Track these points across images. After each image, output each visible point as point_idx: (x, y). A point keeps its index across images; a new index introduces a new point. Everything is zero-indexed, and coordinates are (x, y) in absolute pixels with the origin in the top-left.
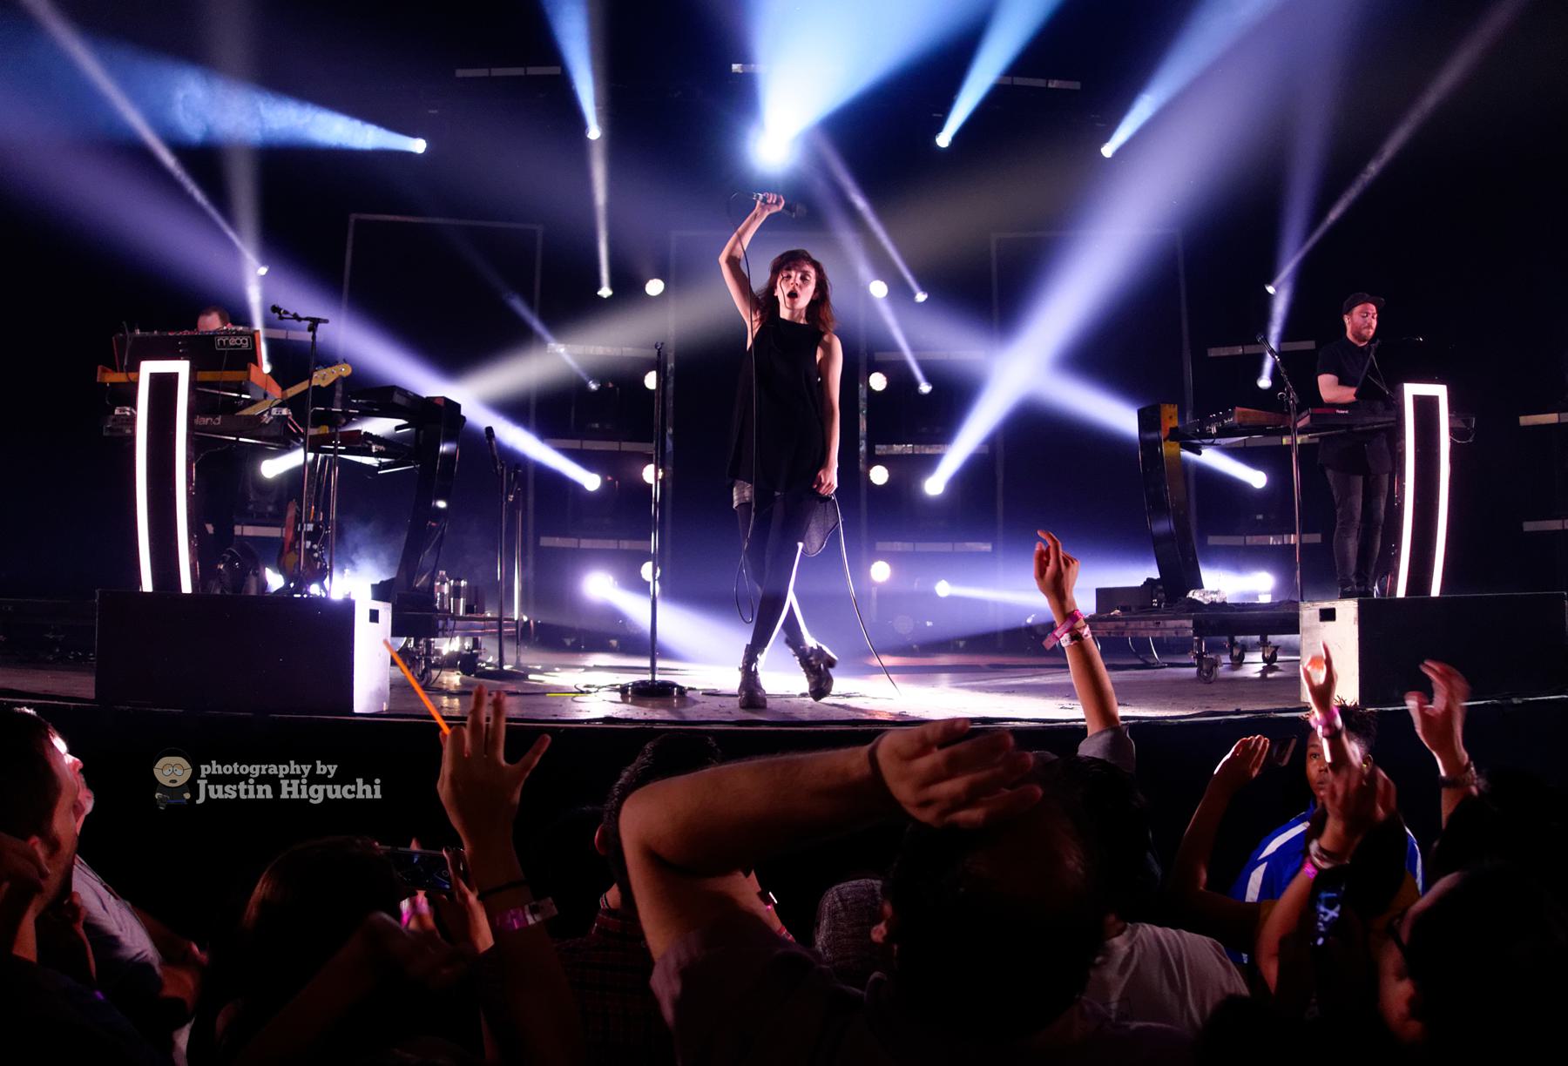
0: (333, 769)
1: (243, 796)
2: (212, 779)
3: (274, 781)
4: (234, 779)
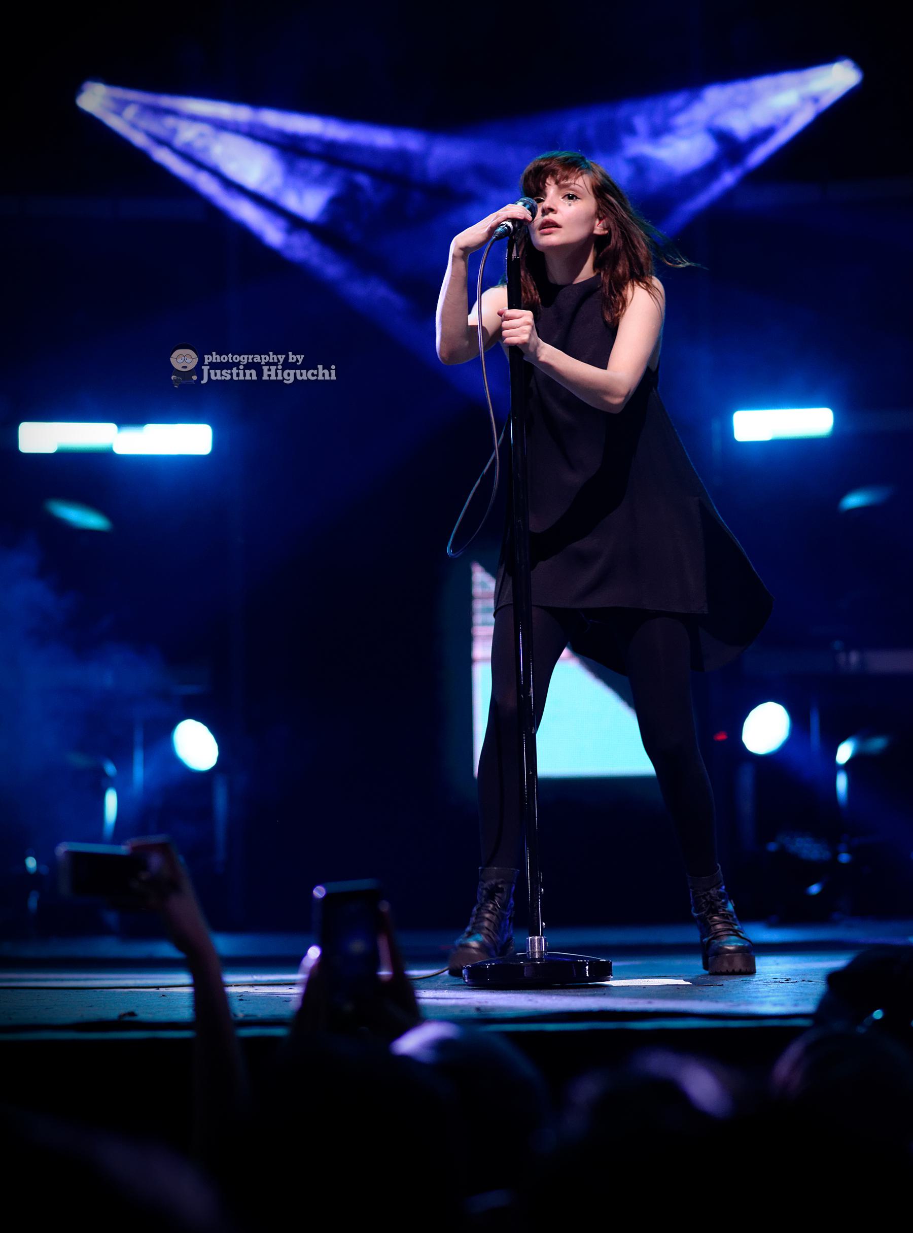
0: (301, 358)
1: (235, 378)
2: (213, 366)
3: (258, 367)
4: (229, 366)
